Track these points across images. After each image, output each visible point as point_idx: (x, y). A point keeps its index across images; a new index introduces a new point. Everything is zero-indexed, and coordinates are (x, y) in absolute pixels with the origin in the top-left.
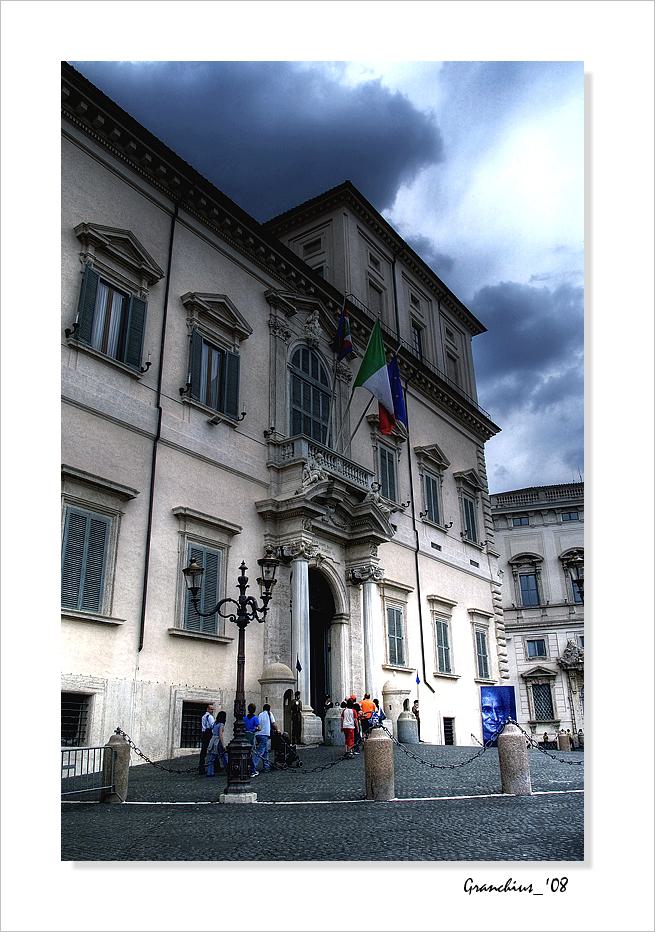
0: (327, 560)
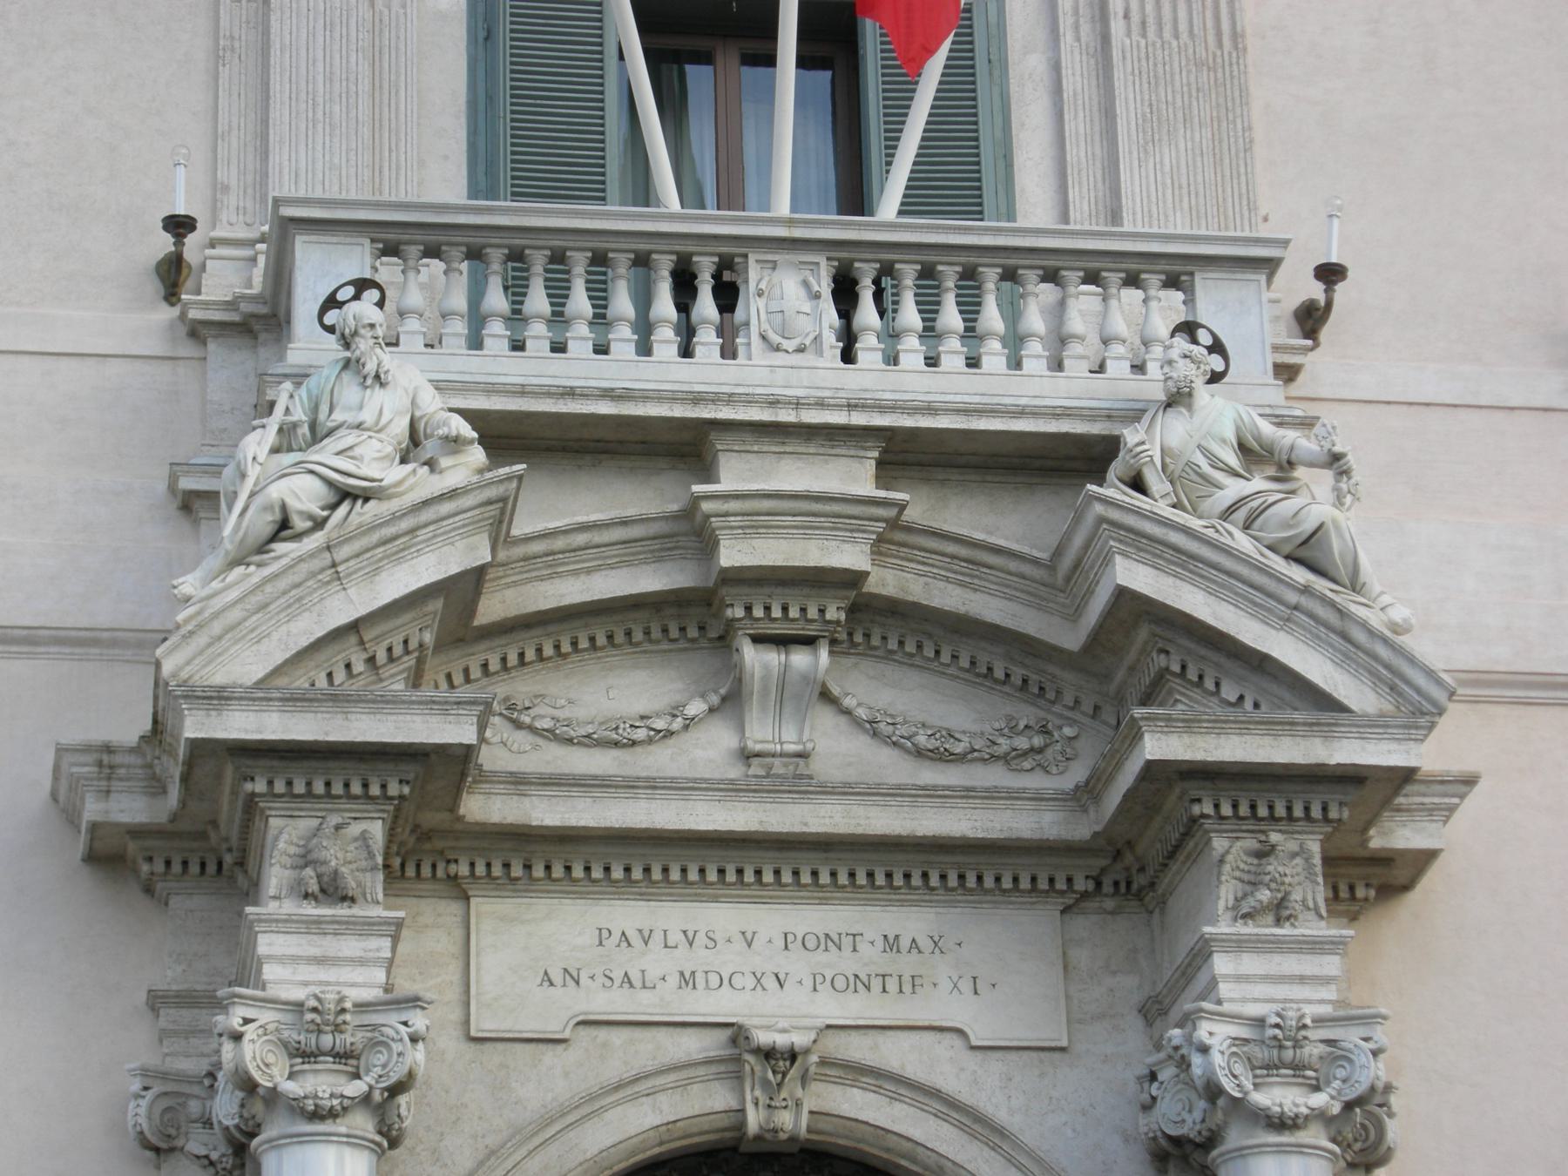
0: (894, 1054)
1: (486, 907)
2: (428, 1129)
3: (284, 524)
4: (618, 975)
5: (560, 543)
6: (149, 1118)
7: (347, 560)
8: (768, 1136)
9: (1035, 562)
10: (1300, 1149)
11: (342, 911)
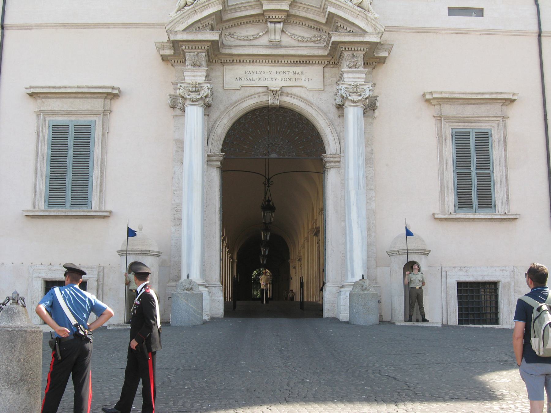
0: (295, 91)
1: (227, 67)
2: (217, 104)
3: (187, 4)
4: (248, 79)
5: (237, 6)
6: (171, 103)
7: (197, 10)
8: (273, 105)
9: (318, 8)
10: (357, 106)
11: (197, 68)
